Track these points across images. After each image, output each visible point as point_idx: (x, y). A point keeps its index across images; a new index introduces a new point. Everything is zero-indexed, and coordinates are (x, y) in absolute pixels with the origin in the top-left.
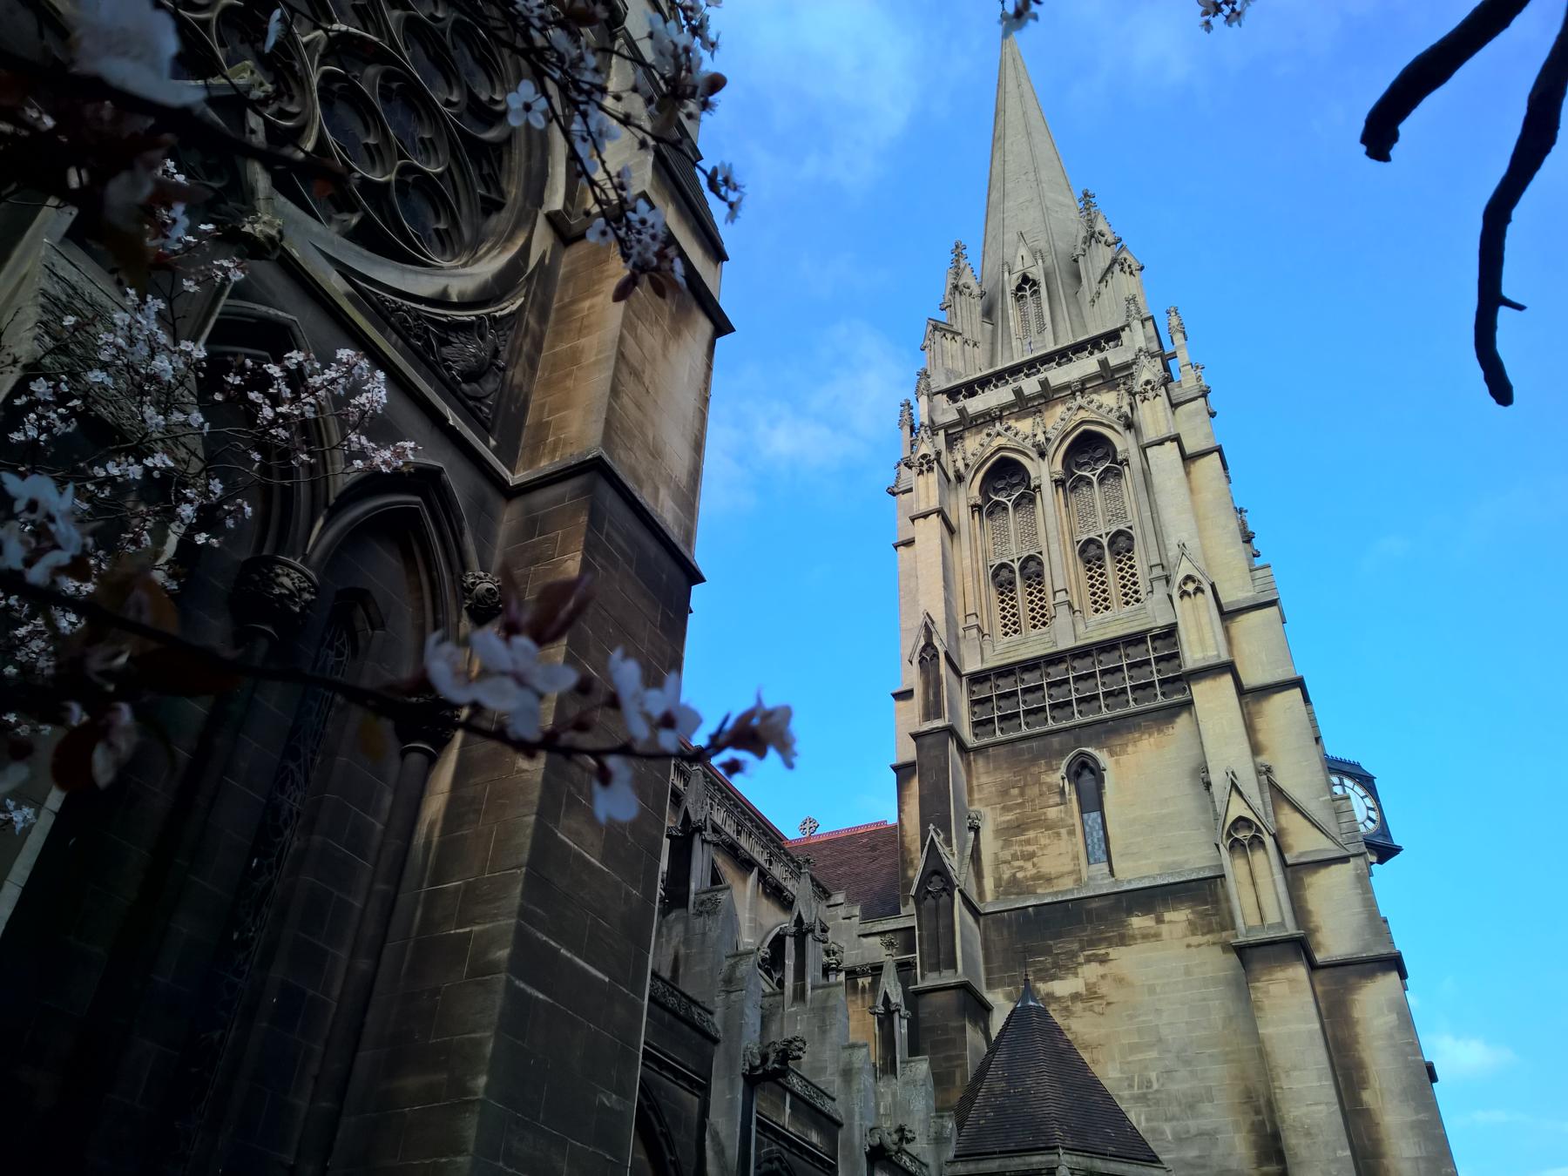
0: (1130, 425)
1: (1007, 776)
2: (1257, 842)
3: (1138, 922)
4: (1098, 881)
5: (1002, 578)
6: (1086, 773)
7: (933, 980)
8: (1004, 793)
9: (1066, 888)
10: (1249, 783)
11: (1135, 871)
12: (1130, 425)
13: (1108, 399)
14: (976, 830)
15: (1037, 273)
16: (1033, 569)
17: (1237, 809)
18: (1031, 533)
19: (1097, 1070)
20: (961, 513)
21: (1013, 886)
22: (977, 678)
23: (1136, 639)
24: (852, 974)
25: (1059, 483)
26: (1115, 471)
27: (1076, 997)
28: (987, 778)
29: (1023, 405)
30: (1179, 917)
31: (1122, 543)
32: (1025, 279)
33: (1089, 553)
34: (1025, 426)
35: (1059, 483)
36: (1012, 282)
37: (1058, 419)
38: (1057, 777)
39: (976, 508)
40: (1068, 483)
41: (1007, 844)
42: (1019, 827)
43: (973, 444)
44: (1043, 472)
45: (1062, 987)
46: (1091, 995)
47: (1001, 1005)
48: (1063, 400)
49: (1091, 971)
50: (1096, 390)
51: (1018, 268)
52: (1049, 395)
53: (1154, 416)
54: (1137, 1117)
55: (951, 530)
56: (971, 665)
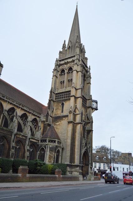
1: (57, 104)
2: (71, 113)
3: (64, 118)
4: (62, 114)
5: (61, 83)
6: (63, 104)
7: (46, 123)
8: (56, 106)
9: (59, 115)
11: (65, 113)
13: (72, 63)
14: (53, 109)
15: (71, 46)
19: (57, 130)
20: (58, 76)
21: (55, 114)
22: (56, 94)
24: (42, 121)
25: (67, 73)
26: (72, 72)
27: (58, 125)
28: (55, 104)
29: (66, 63)
30: (67, 118)
31: (71, 80)
32: (70, 47)
34: (65, 66)
35: (67, 73)
37: (69, 65)
38: (61, 104)
39: (60, 75)
41: (56, 110)
42: (57, 109)
43: (61, 67)
44: (66, 71)
45: (57, 124)
48: (69, 63)
49: (60, 122)
50: (72, 62)
52: (68, 63)
54: (60, 135)
56: (56, 93)
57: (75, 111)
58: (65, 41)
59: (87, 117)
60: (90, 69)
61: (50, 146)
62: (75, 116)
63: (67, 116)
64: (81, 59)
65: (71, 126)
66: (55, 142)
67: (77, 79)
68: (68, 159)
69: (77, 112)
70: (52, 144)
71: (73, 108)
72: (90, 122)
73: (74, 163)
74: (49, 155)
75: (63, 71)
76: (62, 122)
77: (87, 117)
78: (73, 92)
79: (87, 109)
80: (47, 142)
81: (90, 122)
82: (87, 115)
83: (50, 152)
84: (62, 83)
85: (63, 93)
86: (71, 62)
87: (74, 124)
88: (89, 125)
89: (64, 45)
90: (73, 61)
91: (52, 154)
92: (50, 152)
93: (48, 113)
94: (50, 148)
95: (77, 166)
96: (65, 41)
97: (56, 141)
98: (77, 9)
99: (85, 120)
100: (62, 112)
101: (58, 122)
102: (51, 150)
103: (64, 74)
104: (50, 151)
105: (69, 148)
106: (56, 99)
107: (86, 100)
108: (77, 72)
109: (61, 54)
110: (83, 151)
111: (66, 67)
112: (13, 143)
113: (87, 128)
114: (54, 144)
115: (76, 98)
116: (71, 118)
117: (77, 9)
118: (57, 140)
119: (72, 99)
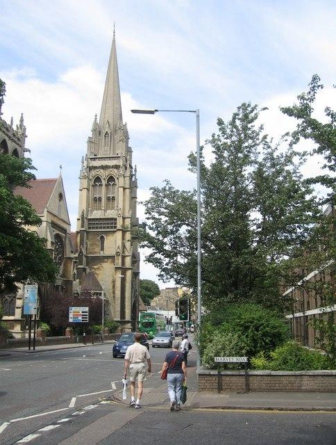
0: (118, 178)
3: (106, 260)
4: (102, 254)
5: (95, 199)
6: (102, 238)
10: (121, 247)
12: (118, 178)
13: (116, 170)
15: (109, 132)
16: (100, 199)
17: (118, 251)
18: (100, 192)
23: (112, 219)
33: (108, 199)
34: (102, 171)
36: (104, 132)
40: (107, 185)
42: (93, 245)
43: (94, 173)
44: (104, 183)
46: (98, 268)
47: (88, 271)
51: (106, 130)
53: (121, 179)
55: (88, 190)
57: (123, 252)
58: (96, 116)
60: (135, 171)
62: (124, 258)
63: (112, 258)
64: (128, 167)
65: (119, 275)
67: (124, 200)
68: (118, 314)
69: (127, 253)
71: (120, 245)
72: (136, 261)
73: (124, 318)
75: (98, 179)
76: (105, 265)
78: (119, 226)
81: (136, 261)
84: (97, 200)
85: (101, 219)
86: (113, 167)
87: (124, 270)
88: (136, 265)
89: (95, 123)
90: (117, 167)
93: (81, 252)
95: (128, 322)
96: (96, 116)
98: (114, 41)
100: (102, 249)
101: (96, 265)
103: (101, 185)
105: (118, 302)
106: (89, 228)
108: (124, 189)
109: (92, 145)
110: (133, 301)
111: (104, 174)
115: (124, 232)
116: (119, 261)
117: (114, 41)
118: (103, 292)
119: (119, 234)
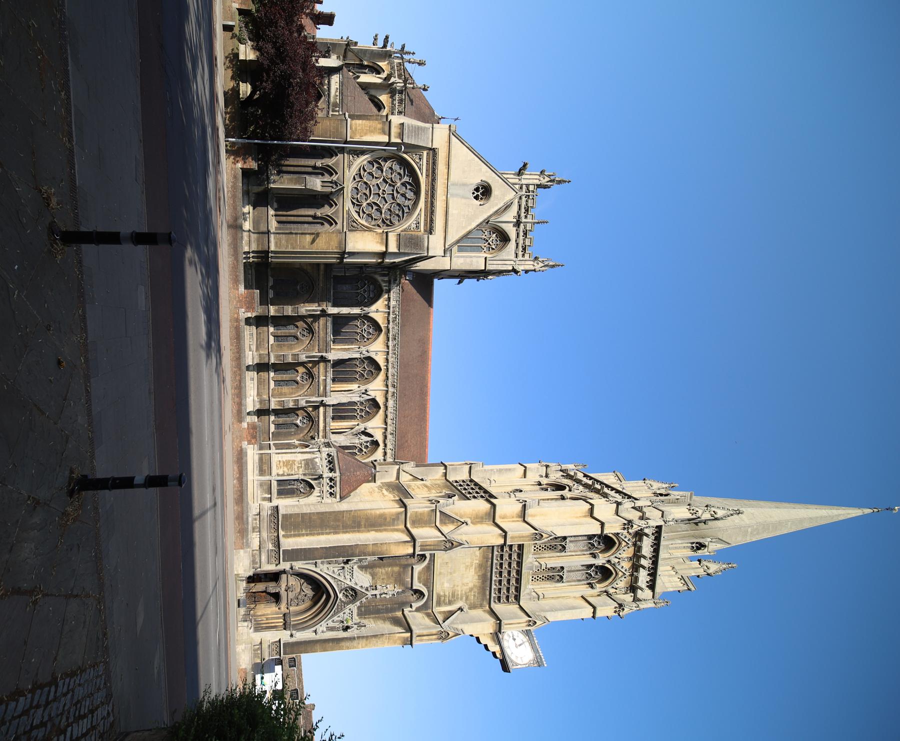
59: (452, 613)
61: (317, 460)
66: (332, 470)
70: (325, 463)
74: (294, 461)
77: (452, 613)
79: (481, 606)
80: (330, 475)
82: (461, 609)
83: (303, 462)
91: (298, 467)
92: (301, 461)
94: (312, 460)
97: (335, 472)
99: (439, 604)
102: (309, 464)
104: (304, 460)
107: (517, 598)
112: (304, 356)
113: (414, 617)
114: (326, 470)
